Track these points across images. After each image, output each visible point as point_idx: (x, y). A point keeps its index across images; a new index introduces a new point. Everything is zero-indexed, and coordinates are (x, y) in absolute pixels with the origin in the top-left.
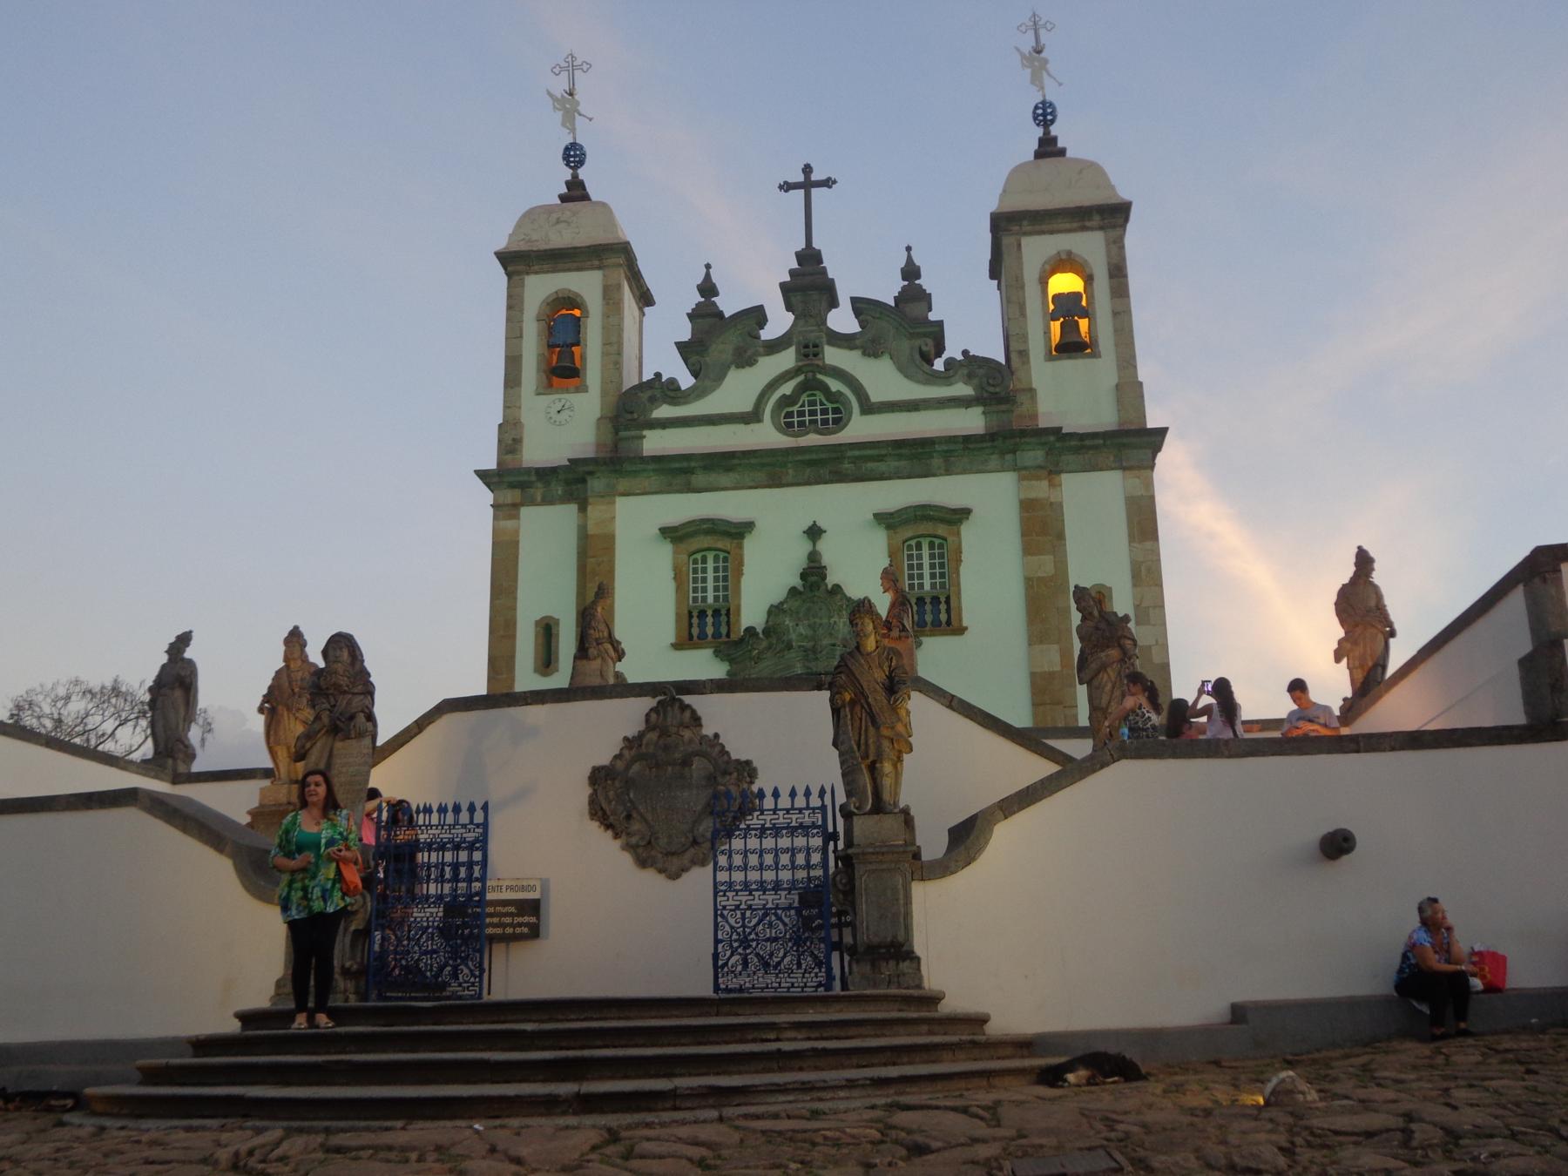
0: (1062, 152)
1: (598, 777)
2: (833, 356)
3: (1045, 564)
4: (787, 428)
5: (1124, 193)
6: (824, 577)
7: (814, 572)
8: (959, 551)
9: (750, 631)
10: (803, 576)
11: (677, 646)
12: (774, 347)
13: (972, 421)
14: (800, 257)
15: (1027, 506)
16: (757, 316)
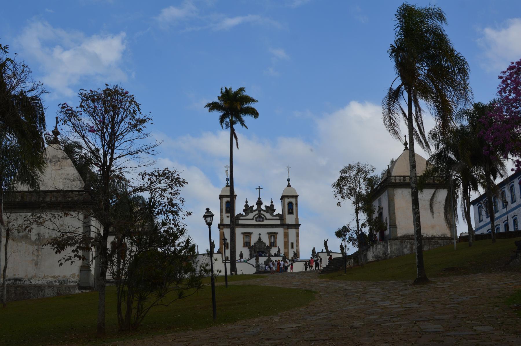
0: (290, 186)
1: (264, 262)
2: (262, 212)
3: (286, 240)
4: (256, 221)
5: (298, 194)
6: (261, 240)
7: (260, 239)
8: (276, 237)
9: (252, 246)
10: (259, 239)
11: (243, 247)
12: (255, 211)
13: (278, 222)
14: (258, 199)
15: (285, 233)
16: (253, 206)
